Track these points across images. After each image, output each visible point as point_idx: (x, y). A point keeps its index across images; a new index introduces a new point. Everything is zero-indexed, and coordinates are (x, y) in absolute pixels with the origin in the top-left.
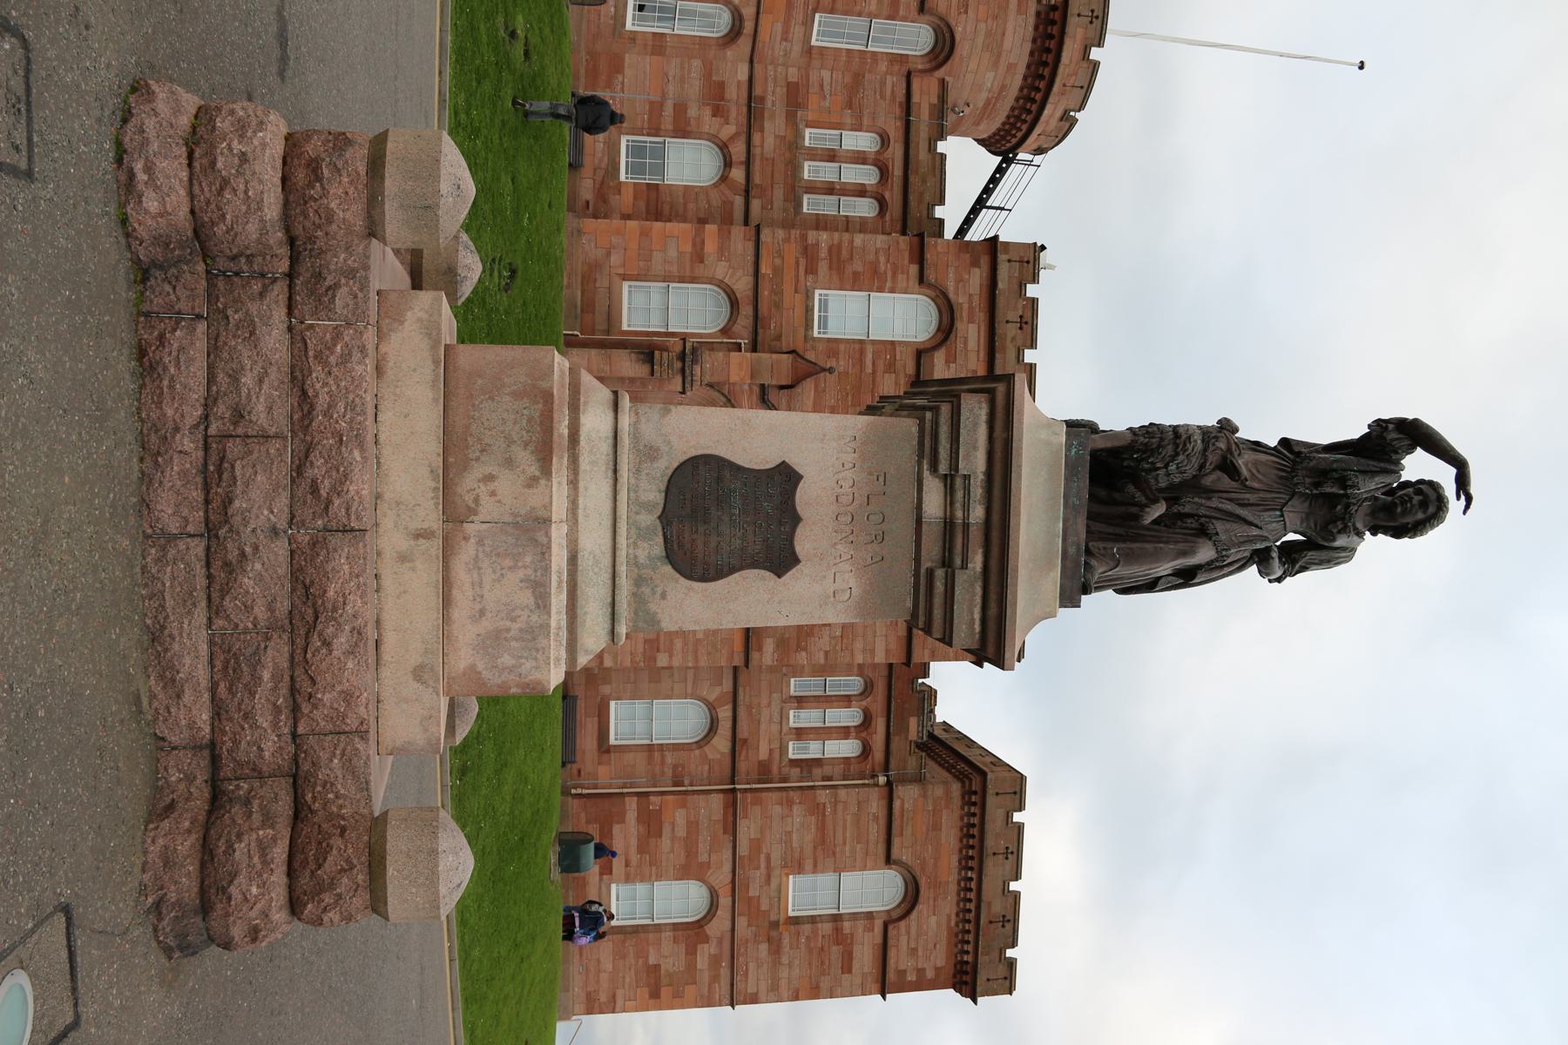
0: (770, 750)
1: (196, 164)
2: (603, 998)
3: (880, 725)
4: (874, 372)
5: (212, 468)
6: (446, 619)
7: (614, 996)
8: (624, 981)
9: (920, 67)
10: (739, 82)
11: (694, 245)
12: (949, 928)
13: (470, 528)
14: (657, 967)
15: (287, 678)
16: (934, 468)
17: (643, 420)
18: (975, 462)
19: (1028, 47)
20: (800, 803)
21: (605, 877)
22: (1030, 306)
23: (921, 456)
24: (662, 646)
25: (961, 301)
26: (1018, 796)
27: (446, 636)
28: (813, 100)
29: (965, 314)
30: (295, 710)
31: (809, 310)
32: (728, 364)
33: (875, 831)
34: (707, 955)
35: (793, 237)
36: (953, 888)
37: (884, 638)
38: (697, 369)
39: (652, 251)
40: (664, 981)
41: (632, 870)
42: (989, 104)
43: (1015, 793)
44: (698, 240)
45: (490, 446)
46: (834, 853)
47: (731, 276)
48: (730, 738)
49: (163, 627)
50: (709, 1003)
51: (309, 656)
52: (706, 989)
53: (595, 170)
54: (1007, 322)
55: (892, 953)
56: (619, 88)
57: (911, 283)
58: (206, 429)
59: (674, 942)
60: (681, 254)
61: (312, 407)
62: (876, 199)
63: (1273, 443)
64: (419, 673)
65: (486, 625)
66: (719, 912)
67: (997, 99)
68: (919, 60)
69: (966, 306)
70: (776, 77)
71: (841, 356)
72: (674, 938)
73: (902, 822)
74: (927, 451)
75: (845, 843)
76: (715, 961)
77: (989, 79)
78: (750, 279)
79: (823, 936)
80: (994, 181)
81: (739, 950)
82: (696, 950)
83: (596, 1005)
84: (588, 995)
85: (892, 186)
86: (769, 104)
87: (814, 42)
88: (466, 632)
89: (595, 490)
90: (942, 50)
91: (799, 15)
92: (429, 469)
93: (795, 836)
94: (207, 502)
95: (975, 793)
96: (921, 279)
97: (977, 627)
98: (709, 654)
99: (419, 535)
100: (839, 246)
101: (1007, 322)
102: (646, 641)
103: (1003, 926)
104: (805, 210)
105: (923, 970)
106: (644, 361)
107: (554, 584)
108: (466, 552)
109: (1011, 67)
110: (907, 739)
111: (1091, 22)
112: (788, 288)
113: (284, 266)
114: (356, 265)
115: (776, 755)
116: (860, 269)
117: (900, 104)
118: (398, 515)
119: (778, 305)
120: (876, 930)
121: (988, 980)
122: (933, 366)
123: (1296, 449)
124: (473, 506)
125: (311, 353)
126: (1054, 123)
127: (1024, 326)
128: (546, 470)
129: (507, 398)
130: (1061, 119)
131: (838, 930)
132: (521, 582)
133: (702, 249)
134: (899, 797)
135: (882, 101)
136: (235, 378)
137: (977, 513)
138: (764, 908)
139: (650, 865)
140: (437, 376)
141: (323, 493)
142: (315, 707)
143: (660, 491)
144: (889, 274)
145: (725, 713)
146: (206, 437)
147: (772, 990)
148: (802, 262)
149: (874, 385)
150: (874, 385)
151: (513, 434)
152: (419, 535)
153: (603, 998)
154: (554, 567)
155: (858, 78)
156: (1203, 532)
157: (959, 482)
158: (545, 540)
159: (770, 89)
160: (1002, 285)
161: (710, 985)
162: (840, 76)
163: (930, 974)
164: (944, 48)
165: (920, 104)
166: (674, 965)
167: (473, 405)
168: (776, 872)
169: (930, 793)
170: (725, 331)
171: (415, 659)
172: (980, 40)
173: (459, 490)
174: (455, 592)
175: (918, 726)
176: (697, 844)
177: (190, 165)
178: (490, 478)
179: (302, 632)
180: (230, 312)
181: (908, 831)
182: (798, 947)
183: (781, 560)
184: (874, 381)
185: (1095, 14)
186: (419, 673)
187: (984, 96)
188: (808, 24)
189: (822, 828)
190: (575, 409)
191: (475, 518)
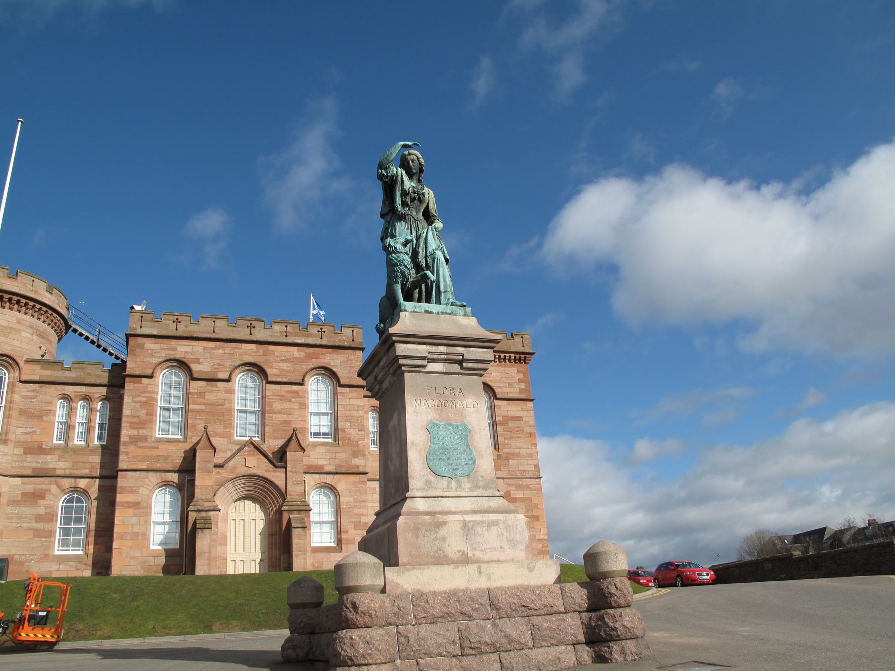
1: (371, 661)
5: (474, 652)
6: (506, 561)
7: (539, 540)
10: (22, 483)
11: (129, 507)
12: (498, 366)
13: (470, 554)
15: (546, 617)
16: (424, 367)
17: (415, 486)
18: (422, 350)
23: (419, 372)
24: (358, 520)
25: (164, 355)
30: (556, 613)
31: (168, 441)
32: (202, 486)
35: (125, 450)
37: (351, 400)
39: (132, 532)
42: (40, 335)
44: (126, 505)
45: (438, 547)
49: (535, 666)
51: (537, 608)
52: (533, 492)
53: (77, 569)
54: (176, 329)
55: (511, 396)
56: (23, 557)
57: (153, 383)
58: (460, 656)
60: (134, 515)
61: (447, 613)
63: (382, 221)
64: (531, 570)
65: (505, 545)
67: (37, 330)
68: (12, 375)
69: (167, 352)
71: (195, 422)
76: (519, 487)
78: (150, 473)
79: (504, 431)
83: (544, 549)
84: (539, 554)
85: (91, 393)
88: (509, 553)
92: (455, 569)
94: (487, 652)
96: (151, 377)
97: (485, 350)
98: (361, 494)
99: (480, 572)
100: (131, 423)
101: (176, 329)
102: (355, 529)
105: (519, 379)
107: (487, 519)
108: (479, 554)
109: (19, 322)
112: (155, 452)
114: (388, 599)
116: (144, 411)
117: (41, 387)
118: (473, 581)
119: (166, 459)
120: (500, 404)
121: (523, 346)
122: (201, 371)
123: (386, 210)
124: (461, 553)
125: (425, 615)
128: (445, 523)
129: (419, 540)
130: (52, 294)
131: (501, 424)
132: (488, 532)
133: (131, 503)
135: (38, 398)
136: (439, 645)
137: (442, 349)
140: (419, 568)
141: (477, 606)
142: (555, 605)
143: (443, 479)
146: (462, 655)
147: (532, 457)
148: (141, 444)
149: (212, 404)
150: (212, 404)
151: (432, 538)
152: (480, 572)
153: (540, 546)
154: (481, 519)
155: (22, 412)
157: (430, 356)
158: (472, 523)
159: (28, 464)
161: (531, 490)
162: (21, 422)
165: (40, 376)
167: (423, 555)
171: (526, 571)
173: (456, 559)
174: (495, 559)
177: (370, 664)
179: (528, 611)
180: (415, 649)
184: (210, 404)
186: (531, 570)
187: (35, 338)
190: (418, 513)
191: (466, 552)
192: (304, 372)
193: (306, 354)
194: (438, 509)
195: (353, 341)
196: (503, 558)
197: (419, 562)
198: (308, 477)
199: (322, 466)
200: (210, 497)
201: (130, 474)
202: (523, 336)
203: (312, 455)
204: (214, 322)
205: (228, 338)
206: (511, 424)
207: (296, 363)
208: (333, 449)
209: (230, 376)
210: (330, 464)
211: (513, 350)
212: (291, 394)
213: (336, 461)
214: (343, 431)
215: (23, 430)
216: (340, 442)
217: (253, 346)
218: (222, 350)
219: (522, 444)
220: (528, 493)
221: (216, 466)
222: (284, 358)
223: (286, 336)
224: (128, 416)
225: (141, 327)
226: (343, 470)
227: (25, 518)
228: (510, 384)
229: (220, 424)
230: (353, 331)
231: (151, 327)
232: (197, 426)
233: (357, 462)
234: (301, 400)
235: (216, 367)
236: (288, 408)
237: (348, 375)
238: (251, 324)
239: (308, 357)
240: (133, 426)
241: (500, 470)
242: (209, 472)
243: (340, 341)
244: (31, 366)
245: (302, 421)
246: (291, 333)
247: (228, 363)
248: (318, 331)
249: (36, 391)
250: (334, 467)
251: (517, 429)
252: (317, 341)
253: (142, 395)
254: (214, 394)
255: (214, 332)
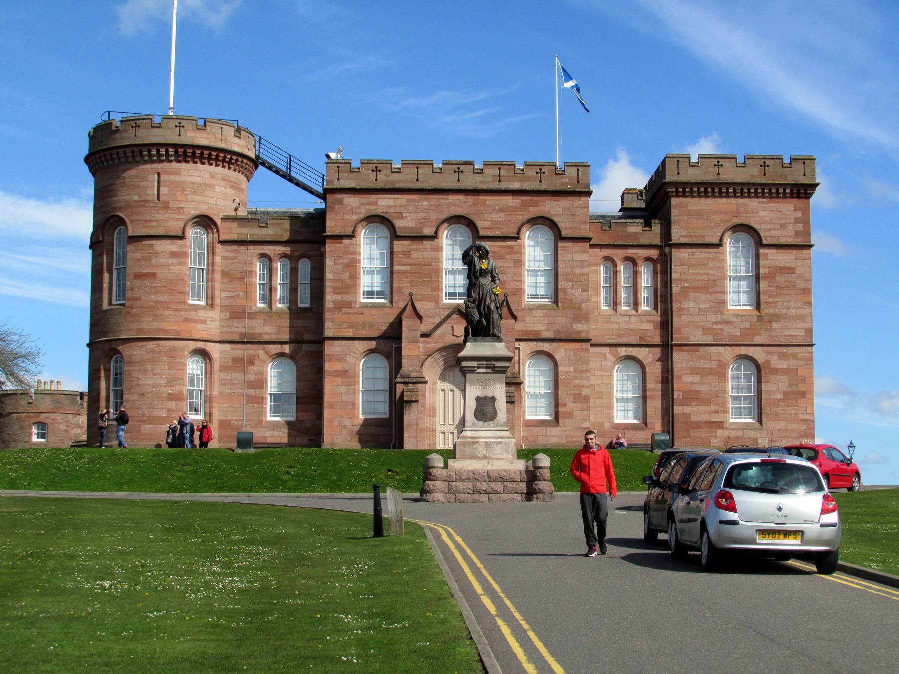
0: (647, 322)
2: (803, 427)
3: (631, 252)
4: (410, 264)
8: (793, 414)
9: (216, 235)
10: (232, 349)
11: (337, 376)
12: (768, 202)
14: (785, 393)
18: (474, 363)
19: (199, 165)
20: (681, 303)
21: (725, 426)
22: (365, 165)
24: (577, 392)
25: (364, 211)
26: (680, 159)
27: (506, 459)
28: (241, 302)
29: (373, 207)
30: (515, 481)
31: (374, 306)
32: (409, 356)
33: (700, 253)
34: (777, 362)
35: (330, 317)
36: (740, 201)
38: (413, 374)
39: (342, 401)
40: (794, 388)
41: (720, 409)
42: (233, 186)
43: (678, 161)
46: (714, 281)
47: (355, 353)
48: (639, 348)
50: (810, 360)
54: (376, 180)
55: (783, 241)
57: (354, 242)
59: (769, 382)
60: (343, 384)
62: (299, 260)
64: (512, 463)
66: (750, 354)
67: (229, 181)
68: (211, 235)
69: (367, 207)
70: (227, 326)
71: (401, 285)
72: (766, 382)
73: (695, 236)
74: (473, 372)
75: (708, 274)
76: (782, 356)
77: (220, 189)
78: (356, 342)
80: (270, 168)
81: (775, 341)
82: (775, 369)
83: (808, 431)
86: (243, 330)
87: (203, 303)
88: (505, 456)
89: (481, 434)
90: (205, 221)
91: (192, 314)
93: (702, 306)
95: (677, 189)
98: (582, 364)
100: (334, 288)
101: (376, 180)
102: (575, 402)
103: (768, 166)
104: (308, 305)
106: (410, 406)
108: (491, 456)
109: (212, 176)
110: (641, 233)
111: (183, 127)
112: (361, 319)
113: (447, 482)
115: (651, 318)
116: (348, 274)
119: (372, 325)
121: (804, 175)
122: (405, 228)
126: (242, 142)
127: (378, 169)
128: (477, 442)
131: (766, 277)
134: (679, 239)
135: (238, 259)
136: (464, 489)
138: (748, 325)
139: (718, 397)
144: (350, 256)
145: (623, 351)
148: (345, 310)
152: (488, 463)
153: (803, 427)
156: (489, 307)
159: (235, 329)
160: (352, 184)
161: (798, 360)
163: (799, 214)
164: (205, 222)
166: (784, 382)
168: (725, 317)
169: (677, 218)
170: (388, 357)
171: (509, 464)
172: (198, 198)
175: (633, 226)
176: (707, 368)
178: (479, 452)
181: (701, 232)
182: (776, 303)
183: (493, 399)
185: (178, 125)
186: (512, 463)
188: (195, 308)
189: (696, 289)
190: (466, 437)
192: (520, 223)
193: (523, 202)
194: (476, 436)
195: (578, 182)
196: (502, 457)
197: (464, 458)
198: (522, 345)
199: (539, 332)
200: (418, 368)
201: (336, 342)
202: (806, 161)
203: (528, 319)
204: (417, 168)
205: (433, 188)
206: (779, 278)
207: (510, 213)
208: (552, 312)
209: (436, 232)
210: (548, 330)
211: (790, 181)
212: (504, 251)
213: (556, 325)
214: (564, 291)
215: (227, 294)
216: (560, 305)
217: (461, 197)
218: (426, 202)
219: (792, 303)
220: (793, 363)
221: (423, 335)
222: (497, 208)
223: (500, 181)
224: (331, 280)
225: (338, 179)
226: (563, 336)
227: (238, 384)
228: (783, 226)
229: (428, 287)
230: (578, 170)
231: (348, 179)
232: (403, 290)
233: (578, 327)
234: (516, 257)
235: (421, 221)
236: (501, 267)
237: (571, 225)
238: (458, 168)
239: (524, 205)
240: (336, 291)
241: (760, 335)
242: (415, 341)
243: (563, 184)
244: (228, 224)
245: (517, 281)
246: (503, 176)
247: (435, 217)
248: (537, 173)
249: (236, 251)
250: (553, 333)
251: (787, 283)
252: (534, 185)
253: (345, 256)
254: (420, 252)
255: (417, 180)
